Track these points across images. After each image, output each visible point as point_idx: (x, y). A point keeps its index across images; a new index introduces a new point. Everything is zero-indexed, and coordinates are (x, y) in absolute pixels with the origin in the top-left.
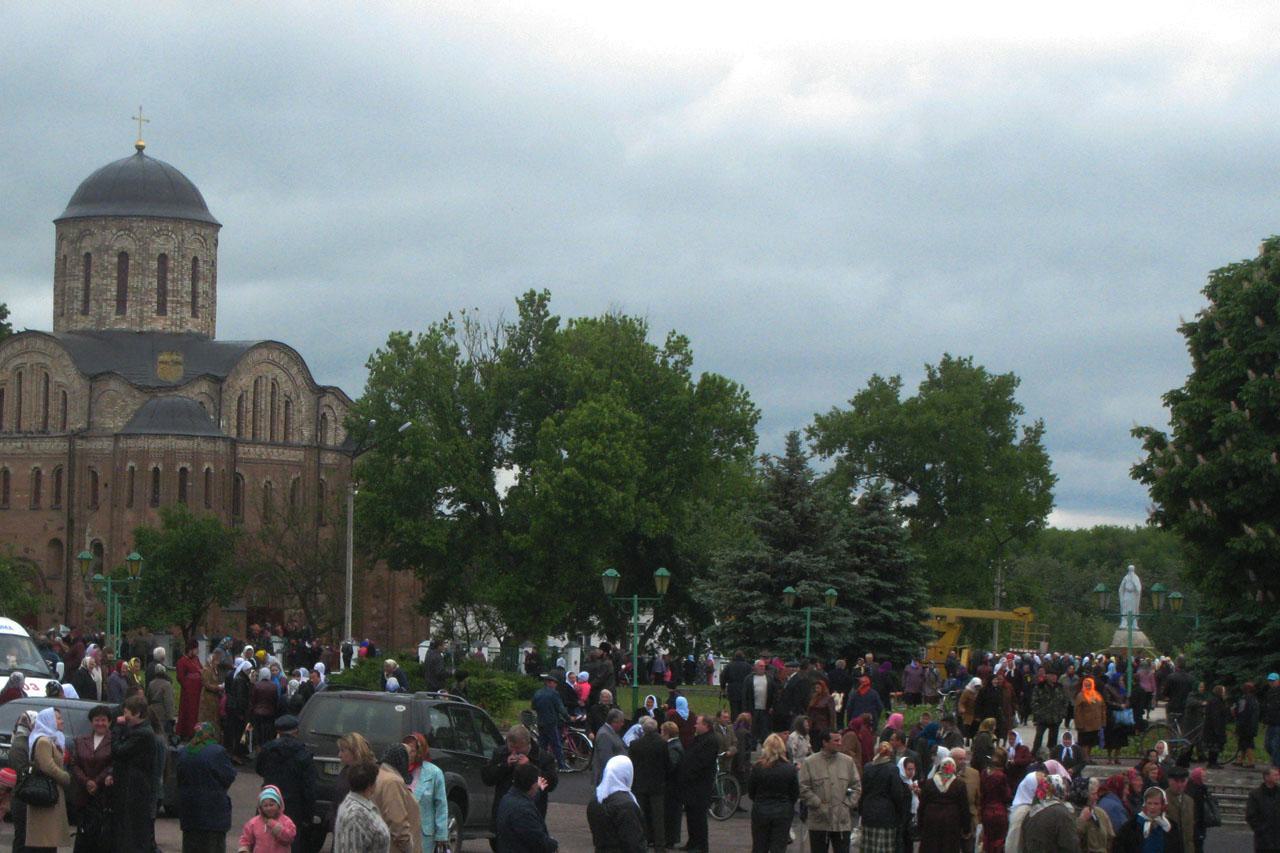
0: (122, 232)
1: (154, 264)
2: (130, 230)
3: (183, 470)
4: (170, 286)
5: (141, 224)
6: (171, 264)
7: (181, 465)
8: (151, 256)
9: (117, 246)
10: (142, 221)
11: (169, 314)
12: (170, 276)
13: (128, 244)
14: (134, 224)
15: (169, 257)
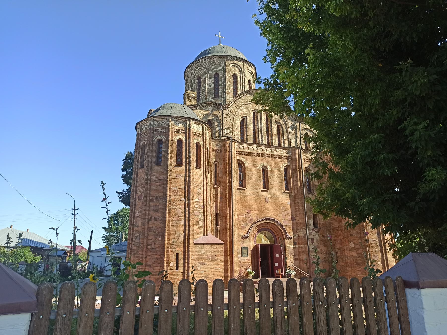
0: (198, 68)
1: (212, 78)
2: (200, 66)
3: (160, 141)
4: (220, 86)
5: (205, 62)
6: (220, 77)
7: (157, 137)
8: (210, 75)
9: (197, 75)
10: (205, 60)
11: (220, 98)
12: (220, 82)
13: (201, 72)
14: (203, 62)
15: (219, 73)
